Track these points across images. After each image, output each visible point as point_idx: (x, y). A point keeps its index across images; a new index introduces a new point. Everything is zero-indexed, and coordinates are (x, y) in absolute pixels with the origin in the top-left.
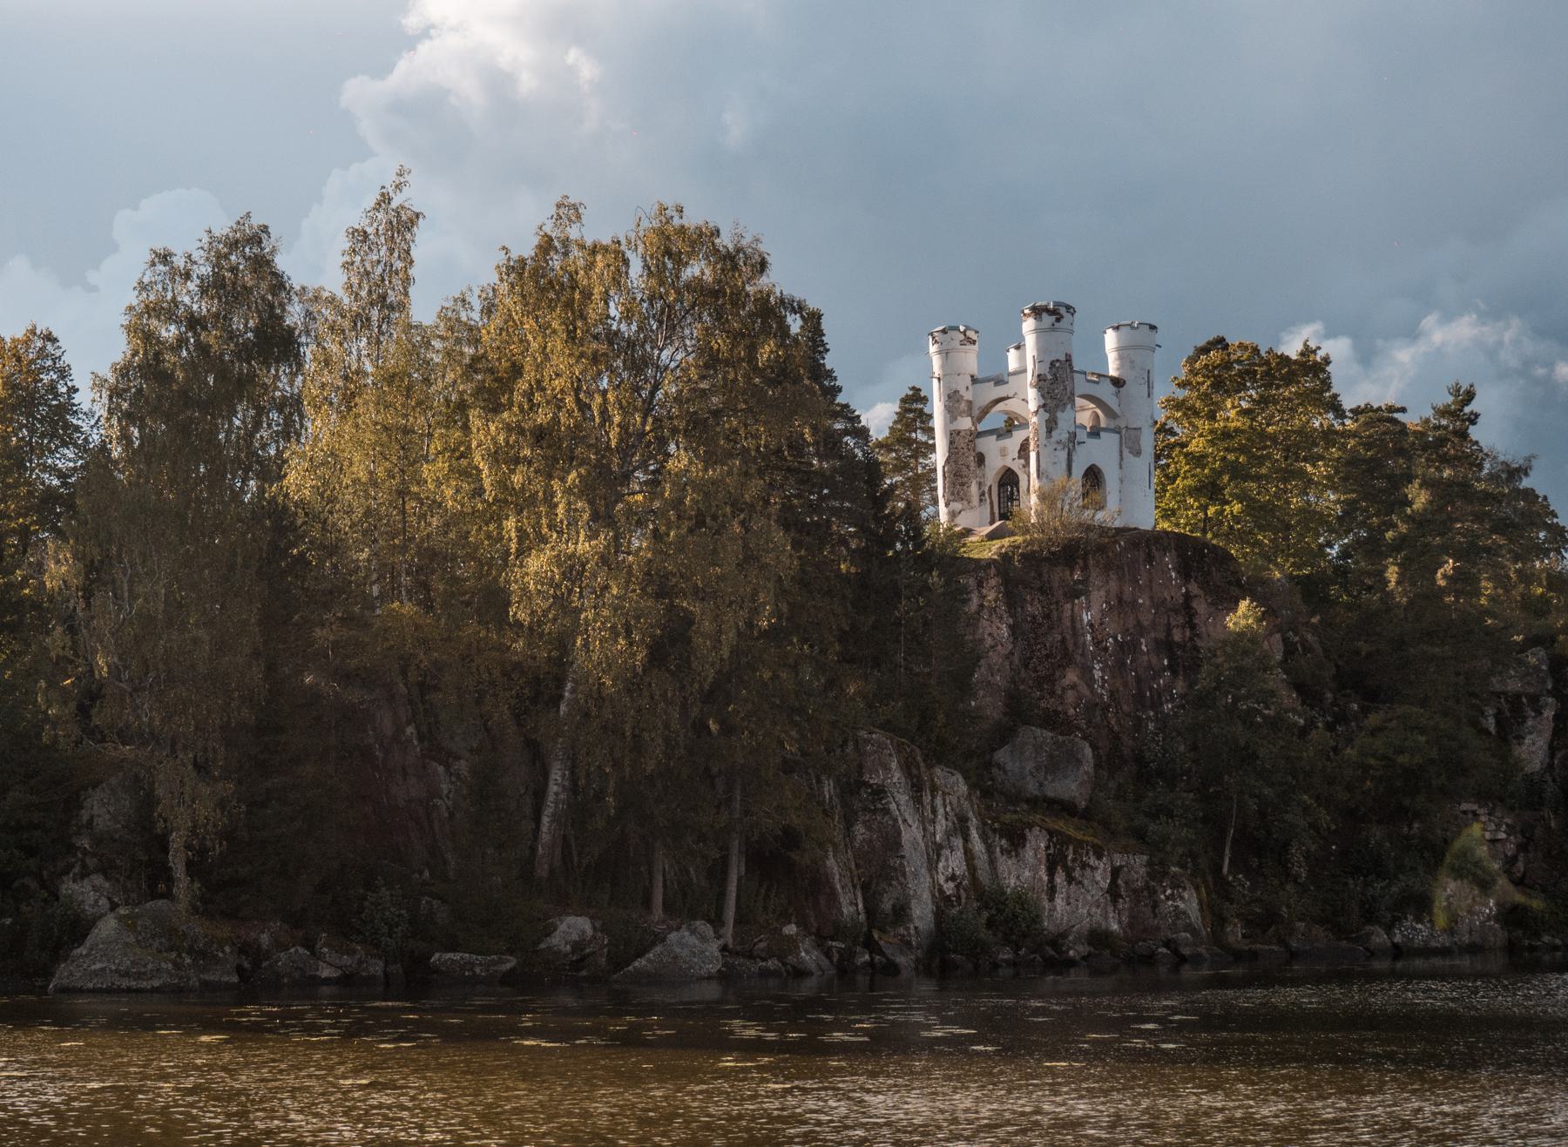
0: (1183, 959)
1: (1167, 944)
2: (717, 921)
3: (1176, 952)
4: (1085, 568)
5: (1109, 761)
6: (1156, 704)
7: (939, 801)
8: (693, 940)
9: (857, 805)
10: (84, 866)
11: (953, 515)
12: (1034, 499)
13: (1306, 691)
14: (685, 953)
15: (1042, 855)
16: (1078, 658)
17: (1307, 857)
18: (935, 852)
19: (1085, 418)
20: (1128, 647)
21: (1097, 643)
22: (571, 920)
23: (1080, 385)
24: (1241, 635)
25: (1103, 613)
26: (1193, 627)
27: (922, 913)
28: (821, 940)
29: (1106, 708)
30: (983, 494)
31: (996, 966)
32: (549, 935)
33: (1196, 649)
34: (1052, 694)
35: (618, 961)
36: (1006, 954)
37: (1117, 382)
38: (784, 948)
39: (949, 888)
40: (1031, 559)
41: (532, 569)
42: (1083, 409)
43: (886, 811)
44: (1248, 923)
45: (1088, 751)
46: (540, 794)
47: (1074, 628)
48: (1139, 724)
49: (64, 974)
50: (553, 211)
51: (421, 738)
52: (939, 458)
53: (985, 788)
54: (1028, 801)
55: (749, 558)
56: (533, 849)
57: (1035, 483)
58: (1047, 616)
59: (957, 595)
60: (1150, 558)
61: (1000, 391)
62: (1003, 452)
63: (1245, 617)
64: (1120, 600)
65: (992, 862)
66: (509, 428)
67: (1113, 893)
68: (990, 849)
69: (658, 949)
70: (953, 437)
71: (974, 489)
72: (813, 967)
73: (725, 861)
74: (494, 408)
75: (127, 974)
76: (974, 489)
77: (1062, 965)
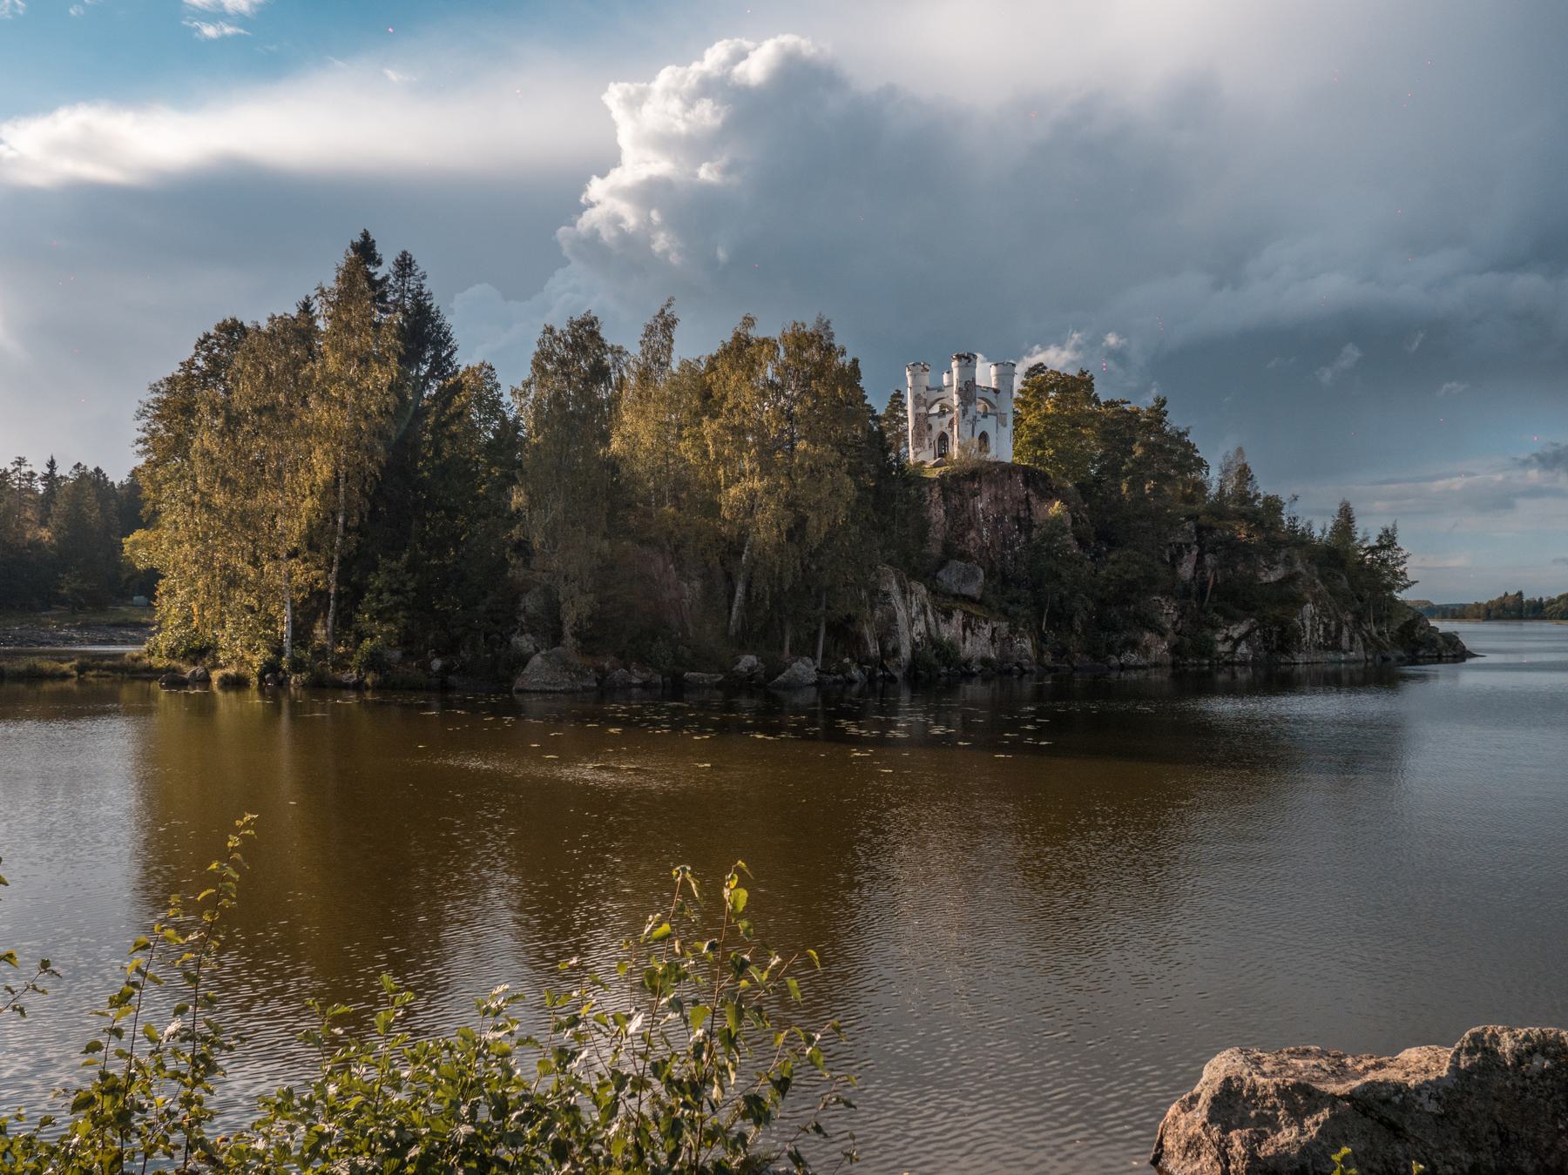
0: (1025, 672)
1: (1017, 664)
2: (814, 657)
3: (1021, 668)
4: (980, 482)
5: (990, 575)
6: (1012, 547)
7: (914, 598)
8: (803, 667)
9: (876, 600)
10: (522, 630)
11: (916, 454)
12: (956, 449)
13: (1082, 543)
14: (800, 673)
15: (960, 622)
16: (976, 525)
17: (1082, 623)
18: (912, 622)
19: (980, 408)
20: (998, 520)
21: (985, 518)
22: (747, 657)
23: (979, 393)
24: (1055, 518)
25: (988, 504)
26: (1030, 510)
27: (906, 651)
28: (860, 666)
29: (988, 550)
31: (939, 676)
32: (737, 664)
33: (1031, 520)
34: (963, 542)
35: (771, 676)
36: (944, 670)
37: (996, 391)
38: (844, 670)
39: (918, 639)
40: (955, 478)
41: (731, 494)
42: (980, 403)
43: (890, 604)
44: (1054, 653)
45: (982, 572)
46: (731, 596)
47: (974, 510)
48: (1004, 556)
49: (519, 683)
50: (741, 320)
51: (676, 570)
52: (911, 424)
53: (934, 591)
54: (953, 596)
55: (835, 492)
56: (728, 623)
57: (956, 440)
58: (962, 506)
59: (921, 497)
60: (1010, 477)
61: (940, 395)
62: (941, 425)
63: (1058, 509)
64: (996, 498)
65: (937, 625)
66: (721, 426)
67: (993, 640)
68: (936, 621)
69: (788, 671)
70: (917, 416)
71: (926, 441)
72: (857, 678)
73: (817, 633)
74: (714, 416)
75: (549, 684)
76: (926, 441)
77: (968, 676)
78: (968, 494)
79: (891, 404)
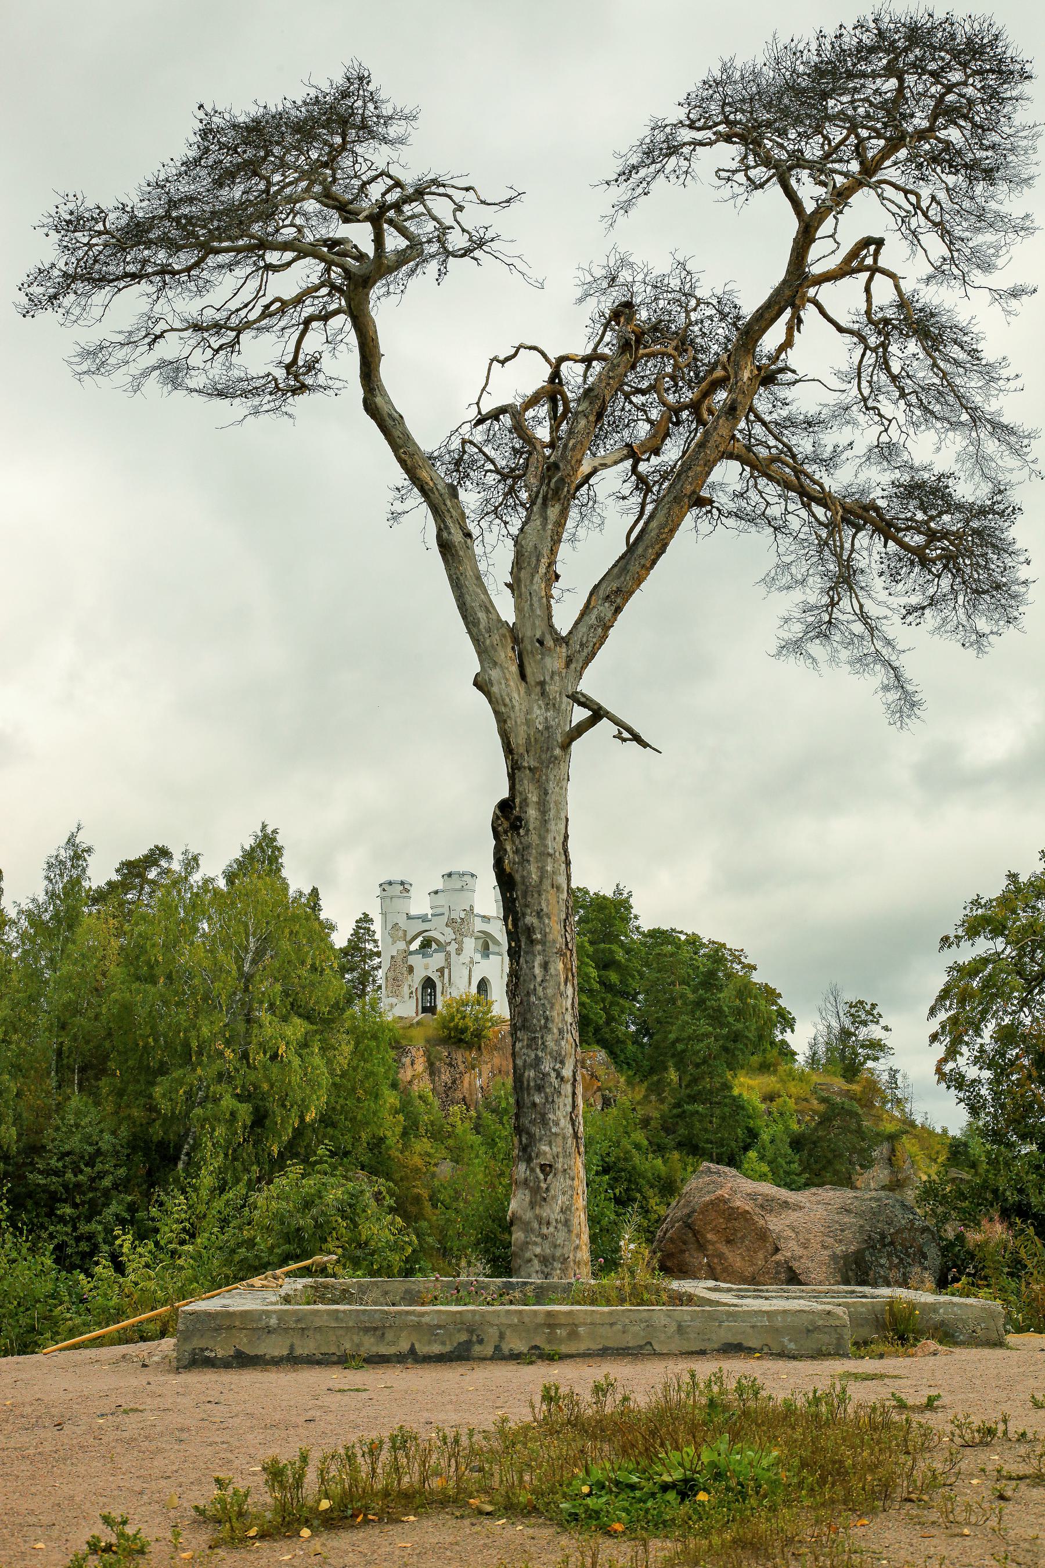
30: (411, 993)
58: (454, 1082)
76: (406, 990)
78: (462, 1067)
79: (356, 933)
